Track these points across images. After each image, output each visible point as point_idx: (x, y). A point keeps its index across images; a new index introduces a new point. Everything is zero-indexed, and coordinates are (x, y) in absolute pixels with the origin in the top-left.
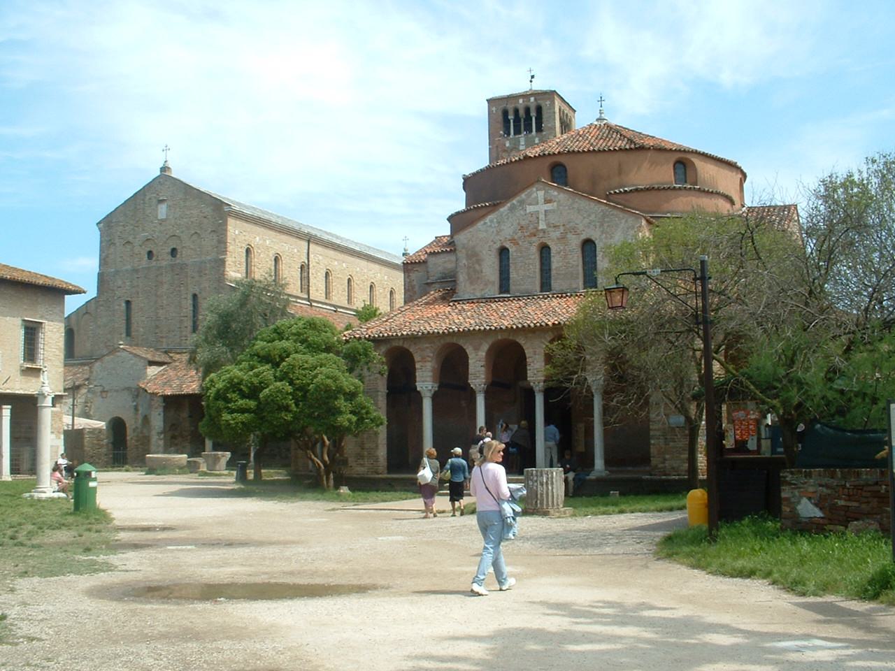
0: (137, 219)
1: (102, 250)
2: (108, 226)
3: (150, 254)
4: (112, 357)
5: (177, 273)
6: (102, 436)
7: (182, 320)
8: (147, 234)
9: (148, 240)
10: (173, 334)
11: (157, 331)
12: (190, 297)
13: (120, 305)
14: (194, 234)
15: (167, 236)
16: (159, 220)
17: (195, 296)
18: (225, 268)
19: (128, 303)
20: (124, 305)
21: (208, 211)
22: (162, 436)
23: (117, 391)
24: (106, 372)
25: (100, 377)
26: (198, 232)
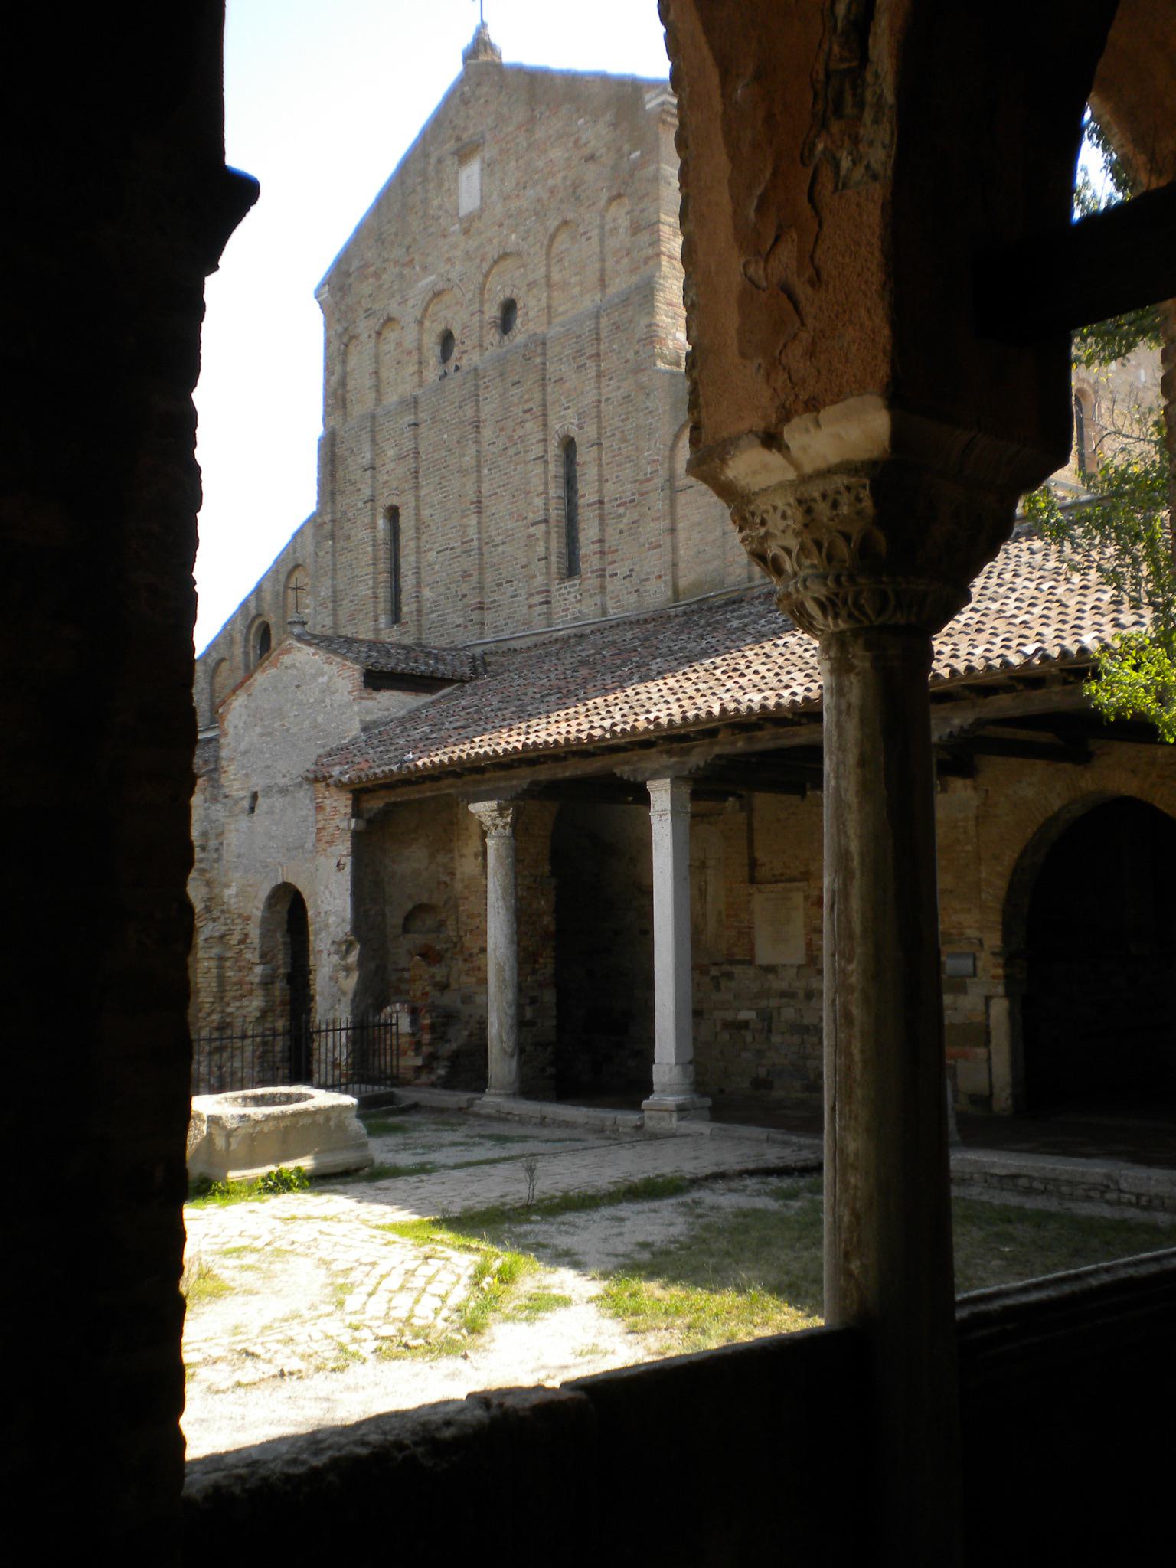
0: (408, 240)
1: (329, 370)
2: (341, 289)
3: (447, 340)
4: (272, 671)
5: (516, 378)
6: (248, 956)
7: (530, 536)
8: (432, 278)
9: (437, 294)
10: (510, 591)
11: (465, 589)
12: (554, 450)
13: (374, 527)
14: (558, 229)
15: (486, 266)
16: (461, 220)
17: (569, 446)
18: (651, 312)
19: (393, 513)
20: (381, 523)
21: (596, 134)
22: (353, 958)
23: (284, 791)
24: (258, 730)
25: (243, 746)
26: (570, 216)
